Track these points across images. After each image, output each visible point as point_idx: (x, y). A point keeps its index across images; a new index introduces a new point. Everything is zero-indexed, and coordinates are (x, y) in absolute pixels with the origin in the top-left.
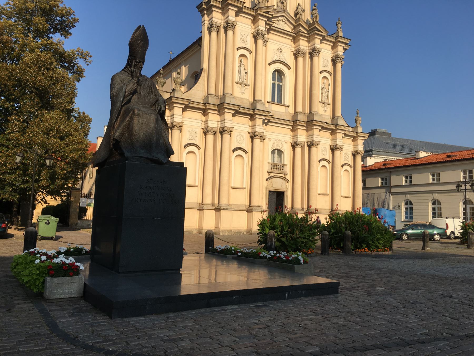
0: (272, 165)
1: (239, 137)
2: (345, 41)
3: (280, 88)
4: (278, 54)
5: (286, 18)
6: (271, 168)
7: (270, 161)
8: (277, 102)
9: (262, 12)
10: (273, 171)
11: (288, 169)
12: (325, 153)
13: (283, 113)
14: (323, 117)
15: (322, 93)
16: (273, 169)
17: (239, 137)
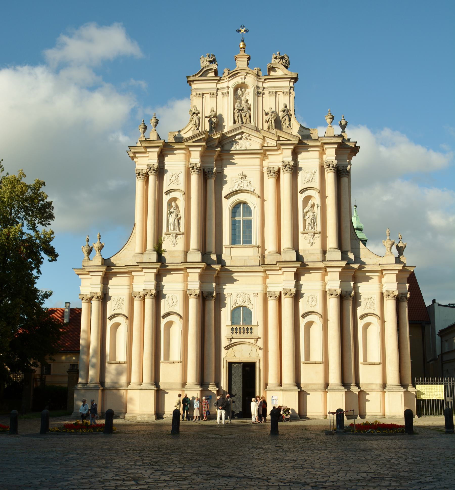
0: (232, 329)
1: (170, 298)
2: (332, 141)
3: (248, 224)
4: (240, 181)
5: (246, 133)
6: (232, 333)
7: (229, 323)
8: (243, 243)
9: (190, 142)
10: (234, 335)
11: (258, 331)
12: (314, 303)
13: (251, 256)
14: (307, 252)
15: (305, 220)
16: (235, 334)
17: (170, 298)
